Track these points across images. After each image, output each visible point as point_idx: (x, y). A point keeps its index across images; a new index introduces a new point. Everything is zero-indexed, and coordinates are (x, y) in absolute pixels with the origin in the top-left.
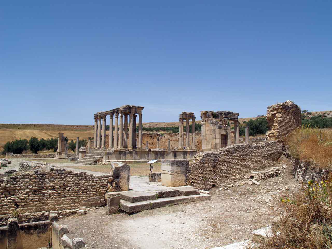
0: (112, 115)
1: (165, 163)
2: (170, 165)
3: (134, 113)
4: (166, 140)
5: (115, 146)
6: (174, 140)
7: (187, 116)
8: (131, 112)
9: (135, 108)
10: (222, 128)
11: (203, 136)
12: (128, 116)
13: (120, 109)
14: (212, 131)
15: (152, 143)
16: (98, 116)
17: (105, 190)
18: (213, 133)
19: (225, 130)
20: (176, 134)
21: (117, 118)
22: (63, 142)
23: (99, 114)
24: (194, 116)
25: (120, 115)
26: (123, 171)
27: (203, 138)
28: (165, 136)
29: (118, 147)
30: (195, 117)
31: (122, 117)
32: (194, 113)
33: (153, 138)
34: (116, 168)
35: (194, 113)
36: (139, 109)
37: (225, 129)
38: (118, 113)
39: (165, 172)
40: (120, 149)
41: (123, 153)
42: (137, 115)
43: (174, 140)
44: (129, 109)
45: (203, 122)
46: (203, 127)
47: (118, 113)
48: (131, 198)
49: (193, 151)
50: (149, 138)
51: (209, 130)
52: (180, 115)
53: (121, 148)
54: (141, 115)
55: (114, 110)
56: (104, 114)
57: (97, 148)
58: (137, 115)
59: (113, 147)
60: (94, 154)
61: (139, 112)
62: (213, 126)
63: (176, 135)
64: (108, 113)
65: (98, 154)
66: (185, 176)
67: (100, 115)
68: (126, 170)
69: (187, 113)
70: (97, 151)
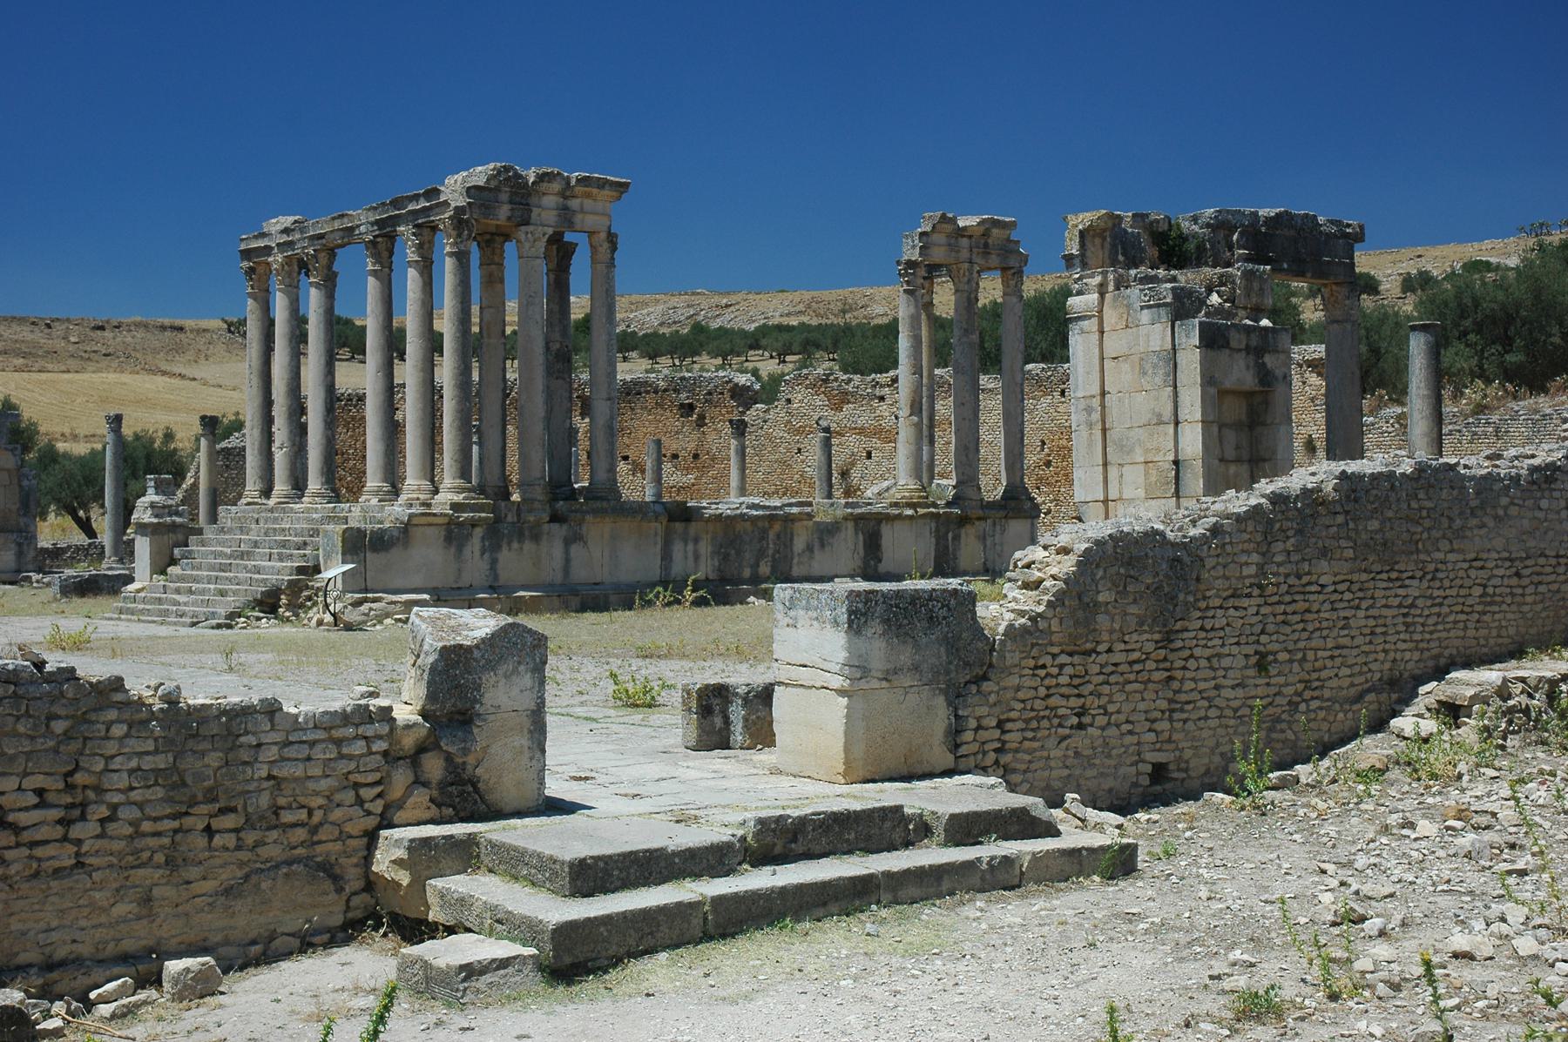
0: (383, 245)
1: (802, 612)
3: (550, 231)
5: (413, 481)
6: (861, 431)
7: (965, 242)
9: (556, 186)
10: (1227, 345)
12: (510, 248)
14: (1155, 366)
15: (696, 456)
17: (369, 813)
18: (1158, 380)
19: (1251, 357)
20: (876, 384)
21: (427, 267)
23: (284, 238)
26: (501, 670)
27: (1083, 417)
29: (436, 491)
31: (461, 257)
33: (702, 417)
34: (444, 647)
36: (588, 195)
37: (1248, 349)
38: (427, 231)
39: (804, 675)
41: (478, 532)
43: (861, 431)
44: (513, 194)
47: (427, 231)
48: (563, 863)
50: (673, 421)
53: (459, 498)
56: (321, 236)
59: (395, 492)
60: (256, 544)
61: (590, 221)
63: (878, 392)
64: (351, 229)
65: (284, 544)
66: (949, 703)
67: (290, 244)
68: (522, 668)
70: (275, 520)
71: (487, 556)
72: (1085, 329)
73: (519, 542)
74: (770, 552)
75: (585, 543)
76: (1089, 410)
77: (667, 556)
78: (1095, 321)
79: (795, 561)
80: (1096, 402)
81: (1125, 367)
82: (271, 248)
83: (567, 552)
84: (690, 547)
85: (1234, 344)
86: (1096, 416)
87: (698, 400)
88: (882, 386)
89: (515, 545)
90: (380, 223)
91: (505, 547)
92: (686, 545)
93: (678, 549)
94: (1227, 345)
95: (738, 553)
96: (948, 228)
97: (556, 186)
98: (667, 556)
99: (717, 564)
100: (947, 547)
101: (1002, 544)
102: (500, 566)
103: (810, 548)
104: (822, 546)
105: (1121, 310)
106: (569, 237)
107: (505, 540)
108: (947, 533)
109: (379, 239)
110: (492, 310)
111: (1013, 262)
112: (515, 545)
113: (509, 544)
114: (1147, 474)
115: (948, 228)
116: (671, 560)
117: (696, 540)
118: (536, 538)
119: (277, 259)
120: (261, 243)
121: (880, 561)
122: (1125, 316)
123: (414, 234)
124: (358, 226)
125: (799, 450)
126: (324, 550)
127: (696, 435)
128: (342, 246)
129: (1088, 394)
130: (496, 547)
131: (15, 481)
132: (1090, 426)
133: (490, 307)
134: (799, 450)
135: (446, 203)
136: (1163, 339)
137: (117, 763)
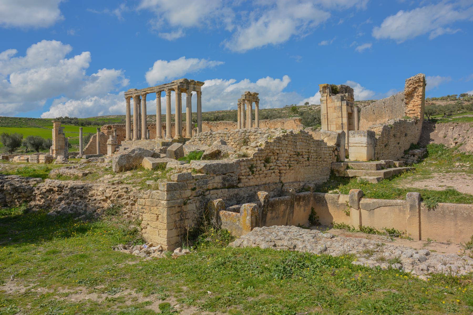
0: (159, 93)
2: (364, 136)
7: (251, 97)
8: (188, 89)
9: (193, 83)
11: (323, 115)
13: (175, 84)
18: (339, 111)
22: (60, 135)
30: (259, 98)
32: (258, 94)
35: (258, 94)
36: (198, 85)
45: (322, 97)
51: (332, 107)
54: (199, 94)
61: (198, 90)
76: (325, 116)
78: (326, 101)
80: (326, 115)
81: (331, 109)
86: (326, 117)
97: (193, 83)
111: (257, 100)
114: (336, 126)
115: (249, 94)
128: (148, 93)
131: (64, 140)
132: (325, 118)
137: (312, 149)
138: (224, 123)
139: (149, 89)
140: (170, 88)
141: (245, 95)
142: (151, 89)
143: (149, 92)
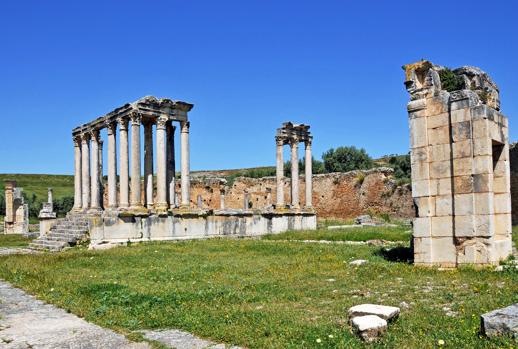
0: (114, 125)
4: (239, 193)
6: (255, 193)
14: (460, 130)
15: (210, 200)
16: (80, 131)
23: (85, 128)
24: (309, 133)
25: (132, 122)
27: (417, 157)
28: (235, 185)
32: (309, 127)
33: (212, 190)
38: (126, 120)
40: (136, 210)
42: (175, 127)
43: (255, 193)
45: (414, 99)
46: (416, 117)
47: (126, 120)
49: (308, 213)
50: (204, 191)
52: (278, 129)
53: (137, 207)
55: (117, 110)
56: (94, 126)
57: (82, 211)
58: (175, 127)
59: (117, 206)
62: (462, 110)
67: (86, 129)
69: (294, 126)
71: (147, 227)
72: (418, 115)
73: (158, 222)
74: (239, 225)
75: (180, 223)
77: (207, 227)
79: (247, 228)
82: (81, 131)
83: (174, 226)
84: (214, 224)
85: (495, 120)
87: (211, 185)
88: (261, 181)
89: (156, 223)
90: (111, 118)
91: (153, 224)
92: (213, 223)
93: (210, 224)
94: (493, 120)
95: (230, 226)
96: (290, 127)
98: (207, 227)
99: (223, 229)
100: (291, 224)
101: (306, 222)
102: (151, 231)
103: (251, 224)
104: (255, 223)
105: (438, 105)
106: (174, 124)
107: (153, 222)
108: (291, 219)
109: (111, 124)
110: (148, 147)
112: (156, 223)
113: (154, 223)
116: (208, 229)
117: (216, 222)
118: (163, 221)
119: (82, 135)
120: (78, 130)
121: (272, 228)
122: (440, 108)
123: (122, 120)
124: (105, 121)
125: (238, 199)
126: (90, 225)
127: (211, 194)
129: (420, 146)
130: (150, 224)
133: (147, 146)
134: (238, 199)
135: (131, 108)
136: (465, 116)
138: (269, 179)
139: (99, 121)
140: (124, 115)
141: (284, 129)
142: (102, 120)
143: (99, 126)
